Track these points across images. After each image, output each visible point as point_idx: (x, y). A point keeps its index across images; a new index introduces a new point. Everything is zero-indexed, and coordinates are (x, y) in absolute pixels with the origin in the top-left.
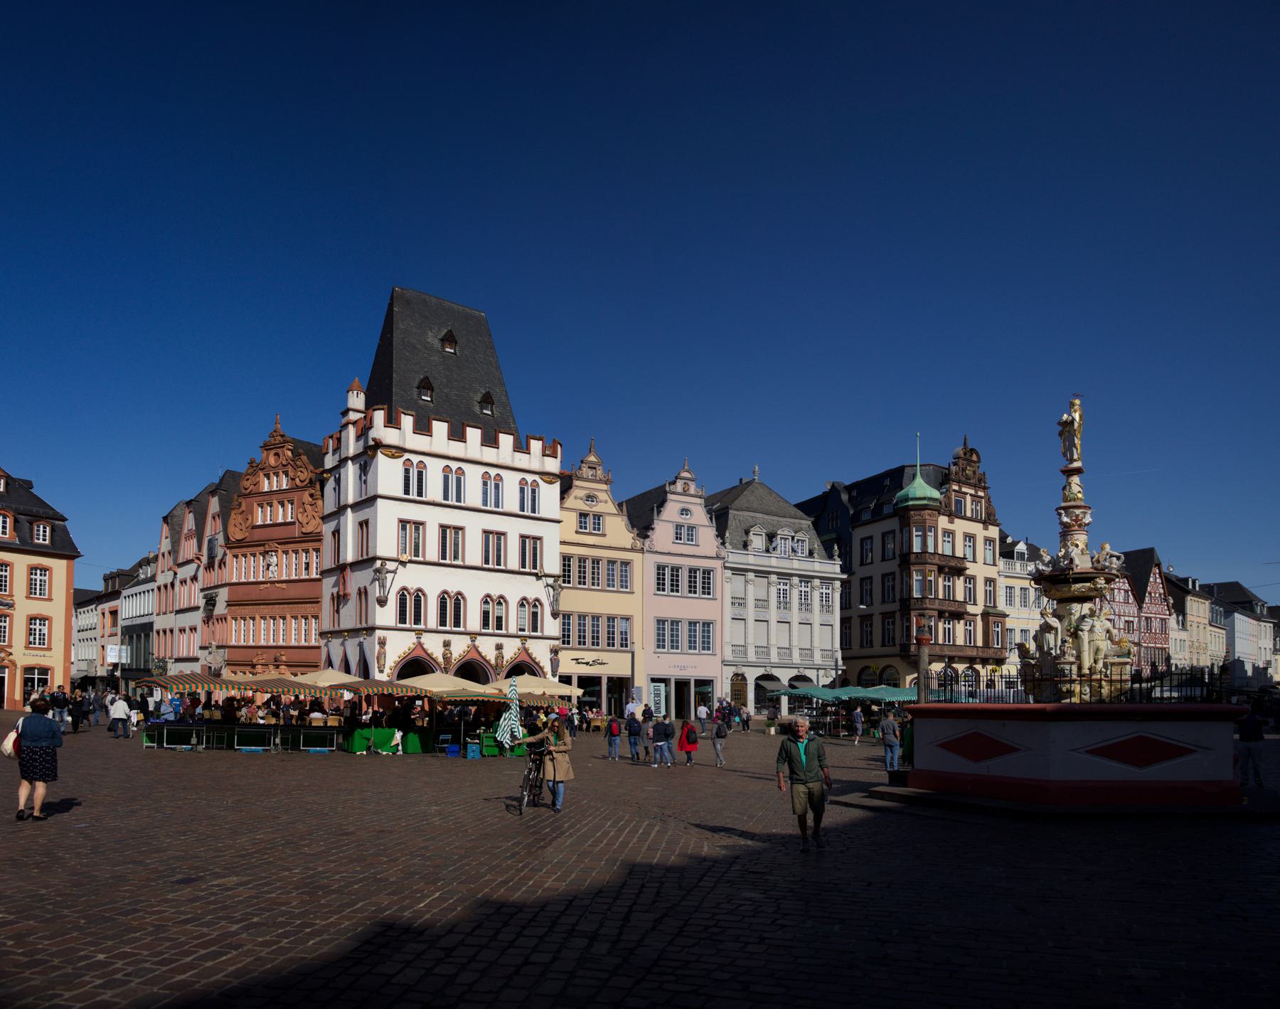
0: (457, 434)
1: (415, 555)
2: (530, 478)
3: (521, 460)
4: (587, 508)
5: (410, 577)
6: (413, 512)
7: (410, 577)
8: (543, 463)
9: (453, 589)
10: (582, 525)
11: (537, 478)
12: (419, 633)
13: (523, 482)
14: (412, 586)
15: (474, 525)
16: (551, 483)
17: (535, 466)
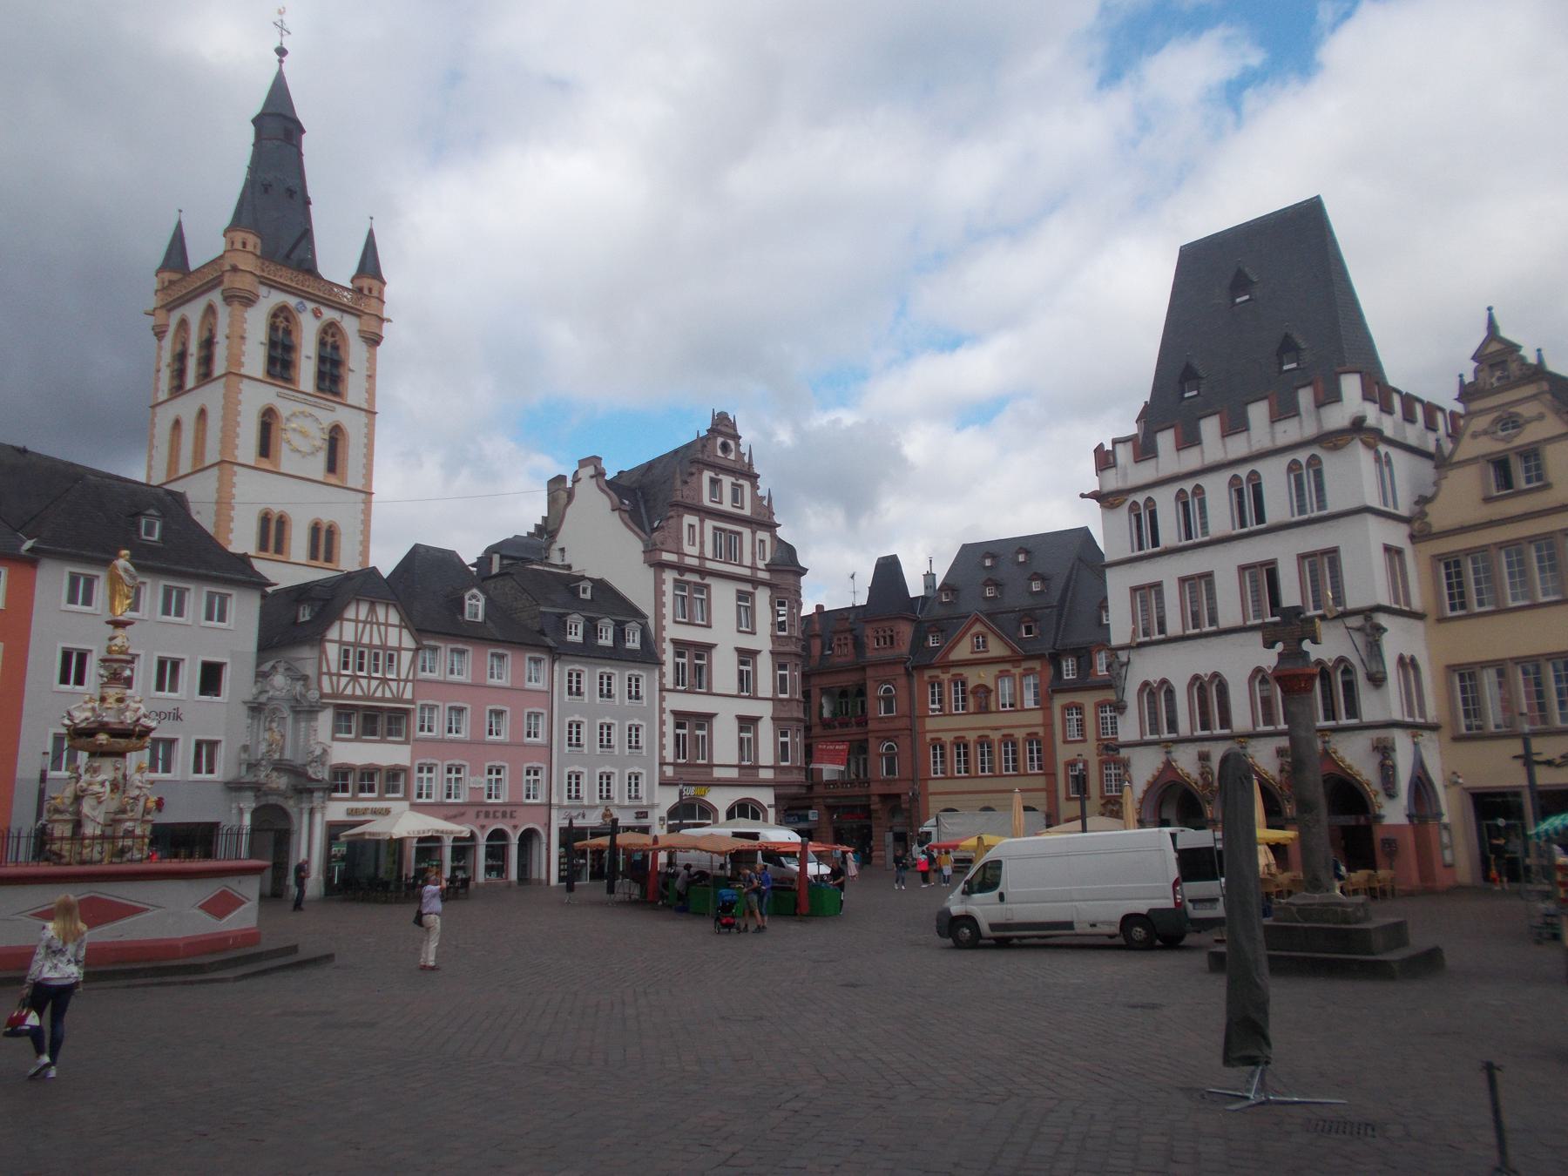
0: (1235, 425)
1: (1153, 636)
2: (1302, 456)
3: (1289, 431)
4: (1500, 446)
5: (1147, 668)
6: (1144, 574)
7: (1147, 668)
8: (1319, 420)
9: (1205, 671)
10: (1505, 480)
11: (1316, 450)
12: (1167, 744)
13: (1294, 467)
14: (1154, 677)
15: (1224, 565)
16: (1336, 448)
17: (1310, 430)
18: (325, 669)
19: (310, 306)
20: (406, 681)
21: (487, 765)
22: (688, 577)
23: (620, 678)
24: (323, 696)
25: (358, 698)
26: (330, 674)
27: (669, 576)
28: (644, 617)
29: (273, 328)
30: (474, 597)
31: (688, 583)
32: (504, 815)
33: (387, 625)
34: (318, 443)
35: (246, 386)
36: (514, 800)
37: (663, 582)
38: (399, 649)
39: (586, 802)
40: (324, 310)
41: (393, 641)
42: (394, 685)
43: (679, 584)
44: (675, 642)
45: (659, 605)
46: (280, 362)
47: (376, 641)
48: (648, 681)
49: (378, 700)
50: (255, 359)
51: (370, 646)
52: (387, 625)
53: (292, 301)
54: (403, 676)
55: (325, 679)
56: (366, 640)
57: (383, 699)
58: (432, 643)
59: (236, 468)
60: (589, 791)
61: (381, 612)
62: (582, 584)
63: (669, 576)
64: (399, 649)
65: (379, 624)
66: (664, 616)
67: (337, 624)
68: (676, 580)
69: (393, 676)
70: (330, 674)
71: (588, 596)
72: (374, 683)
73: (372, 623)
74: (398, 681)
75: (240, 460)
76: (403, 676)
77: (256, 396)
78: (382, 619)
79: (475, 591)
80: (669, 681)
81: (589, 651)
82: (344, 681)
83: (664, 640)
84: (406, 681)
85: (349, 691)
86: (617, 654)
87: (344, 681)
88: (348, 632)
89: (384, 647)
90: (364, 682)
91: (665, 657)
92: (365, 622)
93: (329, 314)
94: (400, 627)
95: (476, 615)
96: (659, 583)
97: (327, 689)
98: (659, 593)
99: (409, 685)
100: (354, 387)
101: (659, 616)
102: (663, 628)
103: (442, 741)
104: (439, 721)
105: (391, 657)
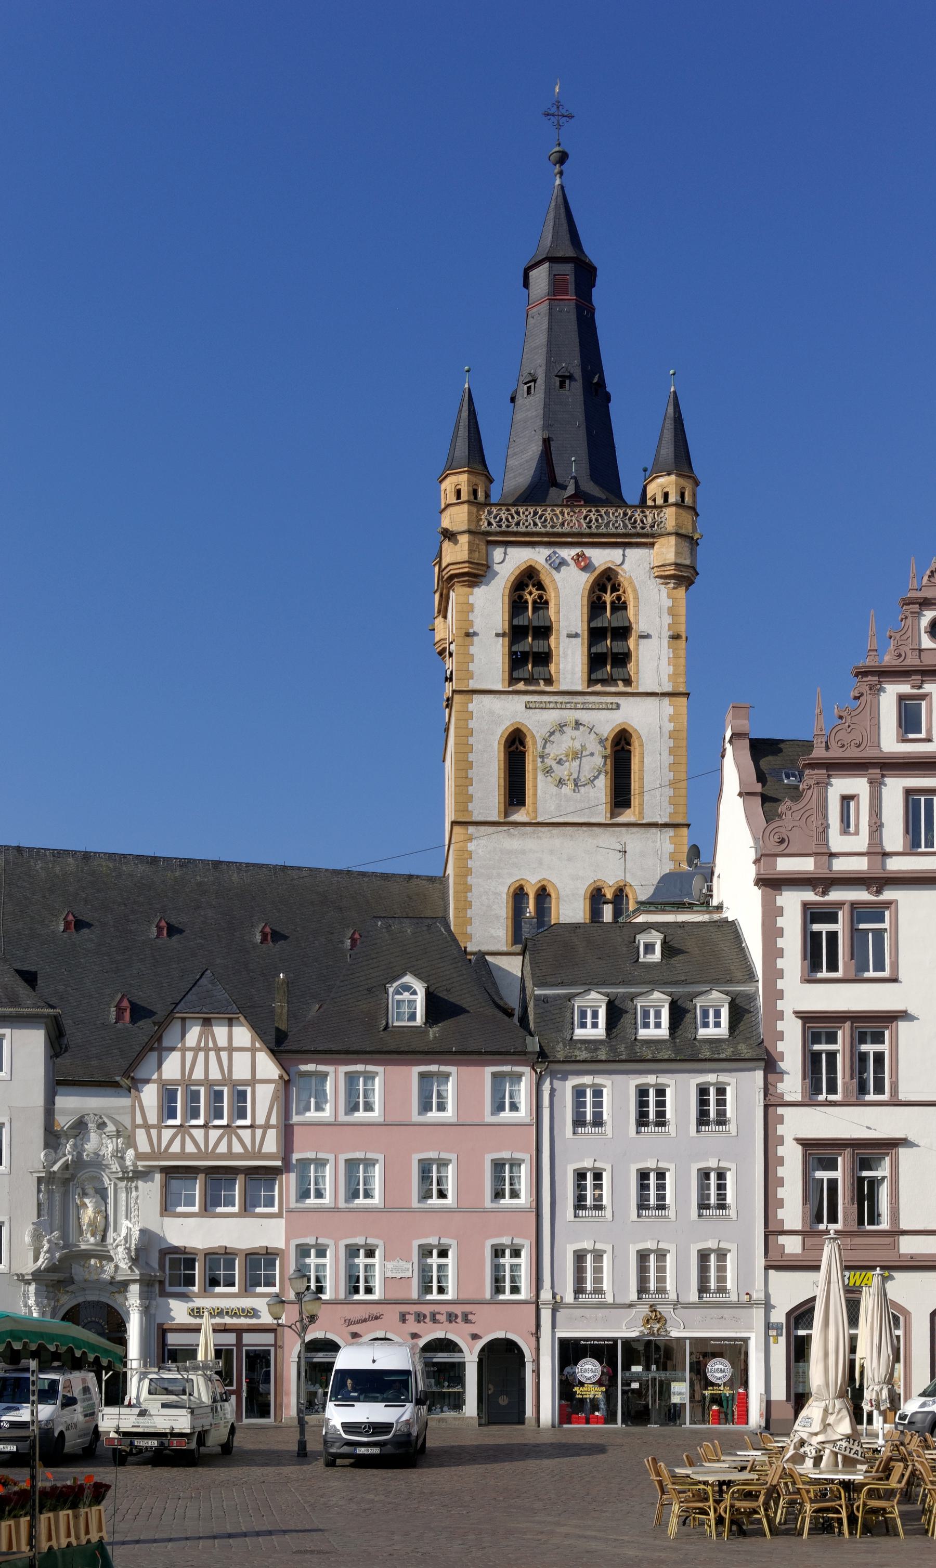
18: (139, 1120)
19: (567, 553)
20: (267, 1126)
21: (416, 1243)
22: (835, 895)
23: (680, 1091)
24: (139, 1156)
25: (191, 1157)
26: (147, 1127)
27: (792, 902)
28: (750, 976)
29: (517, 605)
30: (407, 988)
31: (840, 904)
32: (451, 1318)
33: (231, 1049)
34: (598, 761)
35: (478, 704)
36: (464, 1296)
37: (780, 912)
38: (253, 1081)
39: (609, 1299)
40: (589, 552)
41: (241, 1071)
42: (246, 1135)
43: (813, 914)
44: (806, 1018)
45: (772, 952)
46: (528, 652)
47: (215, 1074)
48: (743, 1089)
49: (222, 1157)
50: (490, 659)
51: (208, 1083)
52: (231, 1049)
53: (538, 556)
54: (260, 1121)
55: (141, 1135)
56: (198, 1074)
57: (230, 1155)
58: (311, 1067)
59: (471, 829)
60: (616, 1279)
61: (220, 1032)
62: (642, 939)
63: (792, 902)
64: (253, 1081)
65: (218, 1050)
66: (780, 974)
67: (154, 1056)
68: (806, 906)
69: (247, 1122)
70: (147, 1127)
71: (657, 956)
72: (214, 1134)
73: (207, 1050)
74: (251, 1127)
75: (476, 817)
76: (260, 1121)
77: (496, 714)
78: (222, 1041)
79: (408, 979)
80: (792, 1084)
81: (621, 1049)
82: (167, 1134)
83: (781, 1015)
84: (267, 1126)
85: (176, 1148)
86: (683, 1051)
87: (167, 1134)
88: (171, 1067)
89: (227, 1080)
90: (199, 1134)
91: (781, 1046)
92: (197, 1050)
93: (601, 557)
94: (253, 1050)
95: (413, 1017)
96: (771, 913)
97: (143, 1146)
98: (771, 932)
99: (272, 1134)
100: (653, 661)
101: (773, 973)
102: (780, 995)
103: (335, 1210)
104: (331, 1179)
105: (242, 1096)
